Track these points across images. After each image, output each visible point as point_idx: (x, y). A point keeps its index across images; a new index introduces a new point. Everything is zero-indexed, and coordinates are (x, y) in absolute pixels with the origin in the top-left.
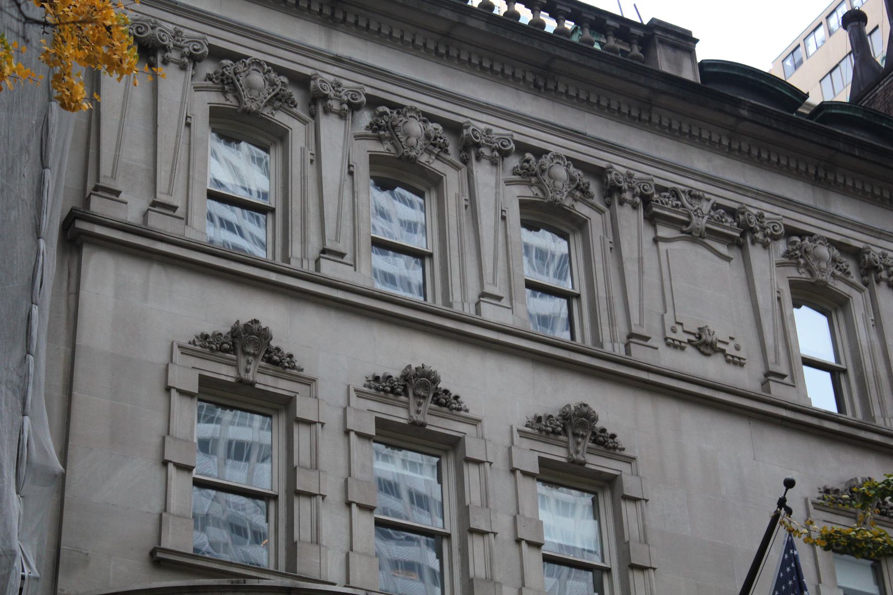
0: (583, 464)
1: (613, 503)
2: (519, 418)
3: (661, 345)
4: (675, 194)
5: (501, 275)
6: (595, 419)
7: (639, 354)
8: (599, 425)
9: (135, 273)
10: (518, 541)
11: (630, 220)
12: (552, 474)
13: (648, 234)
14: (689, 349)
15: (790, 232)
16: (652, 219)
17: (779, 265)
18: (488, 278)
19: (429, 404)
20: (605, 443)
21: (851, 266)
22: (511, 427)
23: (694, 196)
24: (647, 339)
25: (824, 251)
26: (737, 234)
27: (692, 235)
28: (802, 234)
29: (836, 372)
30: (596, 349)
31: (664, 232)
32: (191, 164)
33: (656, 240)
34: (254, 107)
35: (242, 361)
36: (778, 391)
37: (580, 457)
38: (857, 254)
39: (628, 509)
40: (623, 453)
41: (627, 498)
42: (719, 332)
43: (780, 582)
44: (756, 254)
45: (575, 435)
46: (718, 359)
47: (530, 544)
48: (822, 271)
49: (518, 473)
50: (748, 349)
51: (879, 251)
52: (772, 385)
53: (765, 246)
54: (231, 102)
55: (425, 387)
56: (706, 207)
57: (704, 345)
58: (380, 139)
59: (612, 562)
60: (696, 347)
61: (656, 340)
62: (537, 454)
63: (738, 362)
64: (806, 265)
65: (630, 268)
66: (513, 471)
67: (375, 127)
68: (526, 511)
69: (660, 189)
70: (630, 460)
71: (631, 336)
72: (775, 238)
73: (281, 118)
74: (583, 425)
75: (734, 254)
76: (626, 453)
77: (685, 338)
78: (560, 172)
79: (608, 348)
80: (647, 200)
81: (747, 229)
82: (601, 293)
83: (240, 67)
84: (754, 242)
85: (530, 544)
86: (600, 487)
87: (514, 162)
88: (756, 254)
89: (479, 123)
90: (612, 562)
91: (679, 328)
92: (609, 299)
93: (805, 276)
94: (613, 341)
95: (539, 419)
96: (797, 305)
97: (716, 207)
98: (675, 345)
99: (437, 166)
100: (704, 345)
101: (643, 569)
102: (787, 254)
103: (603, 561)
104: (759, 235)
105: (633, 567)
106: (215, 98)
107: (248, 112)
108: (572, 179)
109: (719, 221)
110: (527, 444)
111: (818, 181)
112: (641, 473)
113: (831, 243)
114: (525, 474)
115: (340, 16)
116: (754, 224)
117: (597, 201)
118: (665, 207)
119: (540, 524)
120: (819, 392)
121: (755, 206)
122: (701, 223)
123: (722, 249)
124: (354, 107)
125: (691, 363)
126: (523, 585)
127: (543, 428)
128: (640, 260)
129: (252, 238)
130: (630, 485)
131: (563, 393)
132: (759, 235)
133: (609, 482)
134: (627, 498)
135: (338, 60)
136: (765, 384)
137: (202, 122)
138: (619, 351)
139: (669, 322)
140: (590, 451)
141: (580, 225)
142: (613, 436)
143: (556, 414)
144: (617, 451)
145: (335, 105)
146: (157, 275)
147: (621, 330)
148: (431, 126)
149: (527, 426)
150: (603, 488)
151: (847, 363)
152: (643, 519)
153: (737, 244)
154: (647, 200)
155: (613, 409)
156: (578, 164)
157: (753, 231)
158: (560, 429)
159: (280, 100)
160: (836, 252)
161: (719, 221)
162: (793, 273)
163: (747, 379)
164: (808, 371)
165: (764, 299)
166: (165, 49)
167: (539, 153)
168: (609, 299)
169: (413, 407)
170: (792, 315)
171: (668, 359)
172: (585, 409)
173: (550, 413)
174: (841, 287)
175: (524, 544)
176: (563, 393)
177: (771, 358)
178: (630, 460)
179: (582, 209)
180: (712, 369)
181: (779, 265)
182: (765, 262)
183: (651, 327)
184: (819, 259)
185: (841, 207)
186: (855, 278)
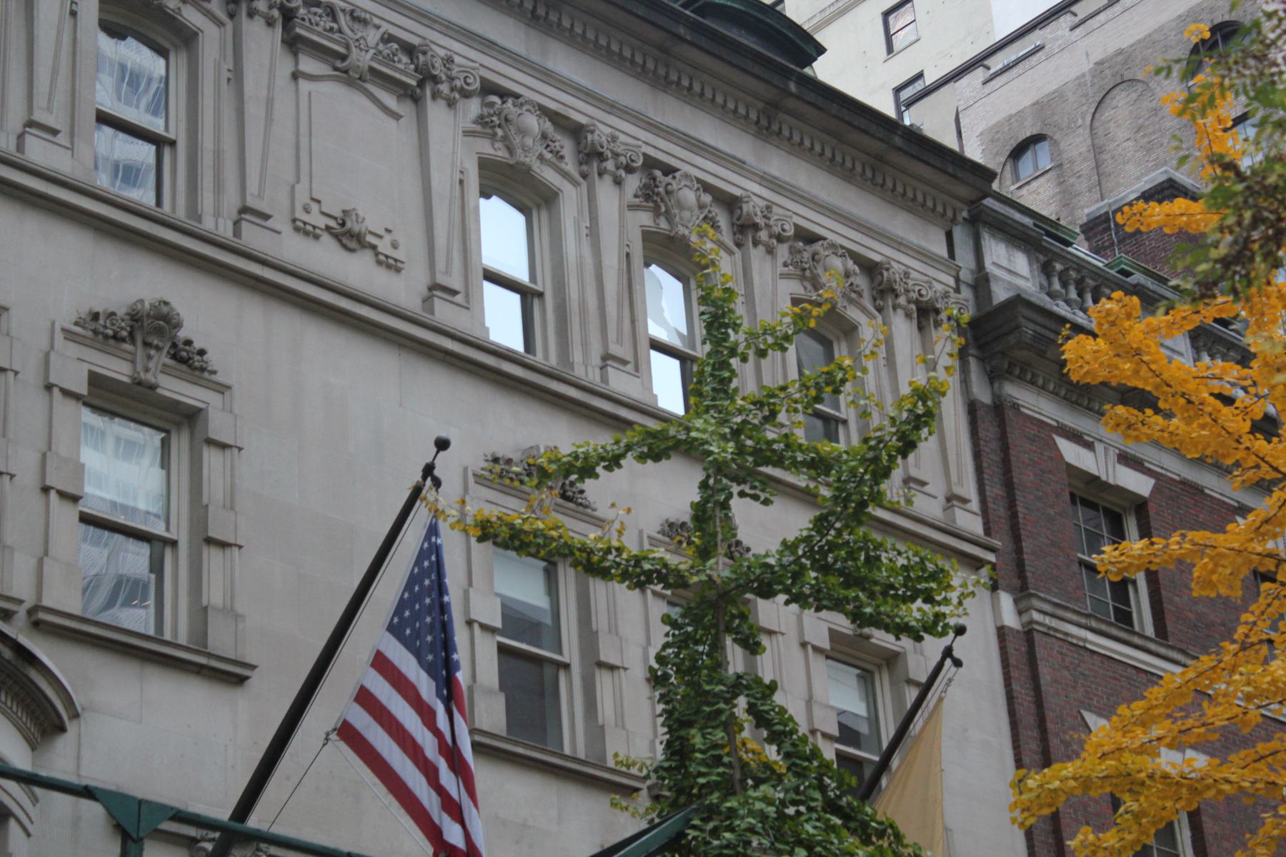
0: (153, 387)
1: (192, 448)
3: (286, 229)
5: (61, 98)
6: (178, 325)
7: (253, 237)
8: (182, 334)
10: (46, 490)
12: (105, 397)
13: (285, 66)
14: (326, 238)
15: (488, 89)
16: (293, 44)
17: (467, 133)
20: (188, 360)
21: (566, 146)
22: (53, 323)
24: (266, 217)
25: (533, 122)
27: (350, 77)
28: (504, 94)
29: (528, 295)
30: (191, 224)
31: (309, 64)
33: (296, 76)
36: (444, 313)
37: (150, 377)
38: (576, 132)
39: (212, 458)
40: (213, 377)
41: (211, 442)
42: (371, 220)
43: (413, 580)
44: (436, 112)
45: (147, 344)
46: (366, 257)
47: (62, 495)
48: (526, 150)
49: (56, 390)
50: (410, 249)
51: (608, 130)
52: (438, 304)
53: (451, 104)
56: (373, 37)
57: (348, 235)
59: (180, 532)
60: (336, 236)
61: (280, 222)
62: (86, 367)
63: (393, 266)
64: (505, 138)
65: (254, 111)
66: (49, 387)
68: (62, 446)
70: (222, 389)
71: (245, 210)
72: (466, 95)
74: (159, 332)
75: (406, 109)
76: (218, 378)
77: (322, 222)
79: (208, 224)
81: (427, 77)
82: (207, 142)
84: (435, 95)
85: (62, 495)
86: (176, 421)
88: (436, 112)
90: (180, 532)
91: (314, 207)
92: (218, 154)
93: (501, 153)
94: (217, 214)
95: (95, 316)
96: (486, 194)
97: (388, 39)
100: (348, 235)
101: (223, 545)
102: (481, 120)
103: (168, 529)
104: (444, 88)
105: (210, 541)
109: (389, 60)
110: (73, 350)
111: (534, 20)
112: (236, 411)
113: (544, 112)
114: (66, 393)
116: (439, 71)
119: (80, 468)
120: (502, 321)
121: (442, 45)
122: (361, 59)
123: (390, 100)
125: (326, 259)
126: (46, 553)
127: (101, 330)
128: (270, 102)
130: (218, 425)
131: (138, 282)
132: (444, 88)
133: (189, 417)
134: (211, 442)
136: (427, 301)
138: (225, 230)
139: (302, 197)
140: (165, 370)
141: (187, 38)
142: (202, 352)
143: (121, 312)
144: (206, 375)
147: (231, 201)
149: (76, 324)
150: (178, 425)
151: (545, 284)
152: (232, 476)
153: (412, 96)
155: (205, 312)
157: (435, 80)
158: (124, 333)
160: (548, 125)
161: (389, 60)
163: (404, 291)
164: (489, 289)
165: (441, 181)
170: (477, 209)
171: (293, 250)
172: (165, 309)
173: (111, 309)
174: (549, 176)
175: (53, 494)
176: (138, 282)
177: (440, 264)
178: (222, 389)
180: (355, 271)
181: (467, 133)
182: (448, 127)
183: (274, 201)
184: (523, 132)
185: (566, 62)
186: (570, 165)
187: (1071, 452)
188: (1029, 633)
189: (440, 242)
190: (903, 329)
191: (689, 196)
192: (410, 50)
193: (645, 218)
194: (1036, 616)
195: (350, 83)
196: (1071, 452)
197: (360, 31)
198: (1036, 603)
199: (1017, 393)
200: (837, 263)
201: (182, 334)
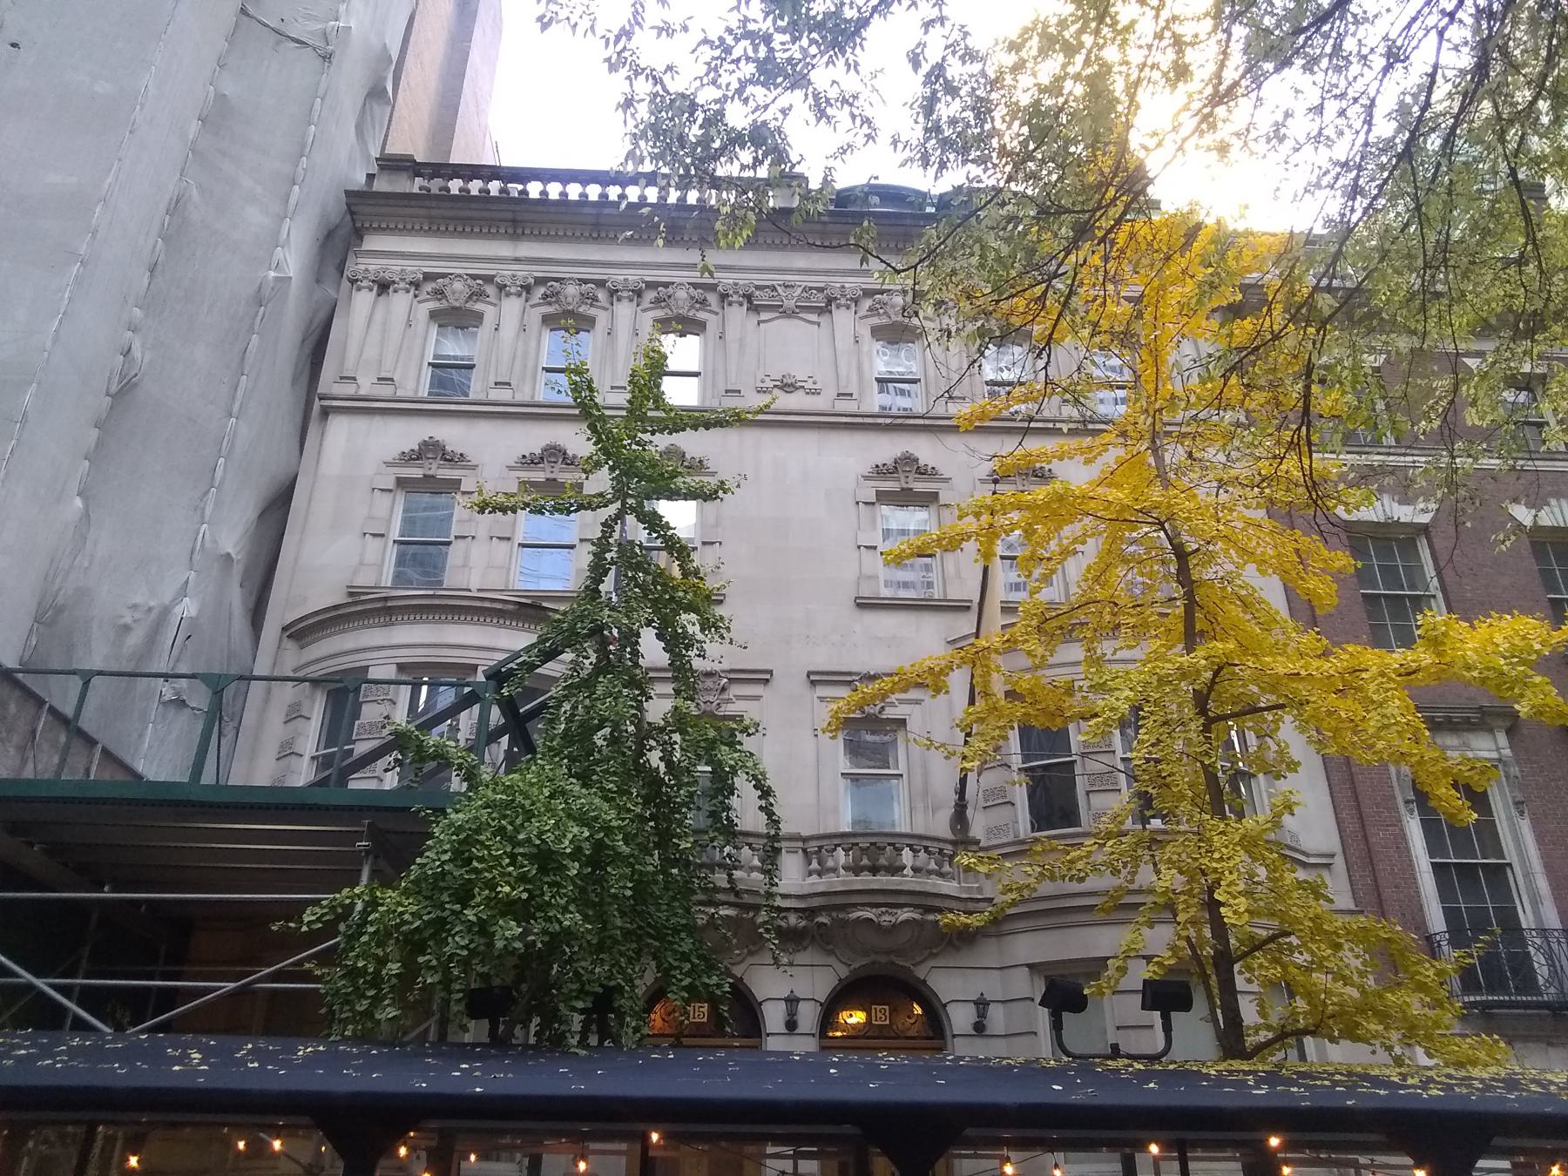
4: (774, 289)
9: (360, 424)
11: (737, 315)
16: (755, 309)
19: (559, 465)
31: (764, 316)
35: (426, 463)
54: (444, 304)
55: (554, 455)
57: (788, 387)
58: (550, 304)
60: (780, 388)
63: (816, 392)
67: (545, 296)
69: (758, 288)
73: (479, 307)
75: (824, 320)
78: (682, 294)
80: (749, 297)
83: (447, 281)
87: (650, 295)
89: (617, 276)
93: (885, 320)
99: (592, 312)
100: (788, 387)
106: (433, 305)
107: (454, 308)
115: (519, 231)
117: (715, 307)
118: (762, 298)
121: (837, 282)
123: (813, 317)
124: (527, 288)
135: (517, 260)
139: (760, 376)
145: (513, 290)
146: (378, 422)
154: (749, 297)
156: (695, 286)
159: (479, 295)
162: (876, 321)
167: (666, 285)
169: (548, 469)
179: (702, 315)
182: (843, 319)
184: (893, 307)
189: (843, 372)
192: (821, 290)
195: (789, 317)
197: (789, 291)
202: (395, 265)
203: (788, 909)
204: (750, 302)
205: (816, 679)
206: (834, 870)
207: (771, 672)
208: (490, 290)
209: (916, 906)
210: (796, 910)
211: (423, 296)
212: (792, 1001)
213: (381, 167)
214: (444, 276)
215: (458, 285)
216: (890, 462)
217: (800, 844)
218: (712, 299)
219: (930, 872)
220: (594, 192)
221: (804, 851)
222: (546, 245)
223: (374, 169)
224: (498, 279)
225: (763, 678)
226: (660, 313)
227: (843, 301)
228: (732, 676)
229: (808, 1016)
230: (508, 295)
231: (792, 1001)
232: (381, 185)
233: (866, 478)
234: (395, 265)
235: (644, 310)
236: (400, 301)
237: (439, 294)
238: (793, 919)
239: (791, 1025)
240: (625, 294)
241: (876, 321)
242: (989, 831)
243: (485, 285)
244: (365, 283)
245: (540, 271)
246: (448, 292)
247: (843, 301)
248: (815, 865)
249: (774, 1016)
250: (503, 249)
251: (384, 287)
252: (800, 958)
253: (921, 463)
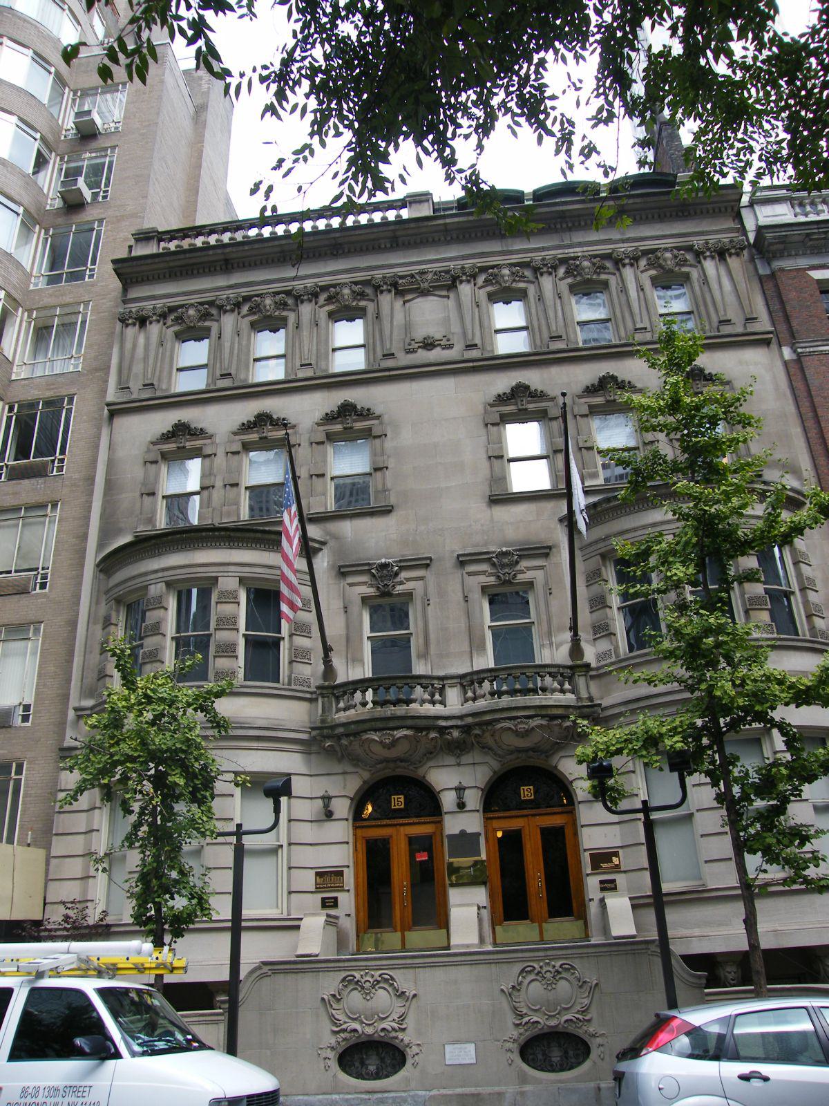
2: (318, 415)
4: (412, 276)
11: (386, 299)
14: (420, 350)
16: (400, 293)
18: (638, 319)
23: (422, 273)
26: (449, 283)
28: (493, 267)
32: (647, 305)
34: (192, 325)
46: (438, 349)
48: (505, 282)
57: (428, 344)
58: (255, 313)
63: (450, 347)
64: (497, 282)
67: (251, 309)
77: (417, 345)
78: (346, 291)
80: (395, 285)
83: (184, 310)
84: (461, 282)
98: (409, 352)
100: (428, 344)
108: (354, 292)
117: (371, 296)
123: (444, 293)
125: (423, 356)
129: (608, 336)
135: (230, 287)
137: (648, 284)
139: (408, 341)
148: (278, 298)
159: (206, 316)
161: (438, 280)
162: (489, 289)
166: (149, 317)
167: (334, 286)
168: (623, 317)
171: (404, 359)
180: (436, 355)
187: (817, 275)
188: (799, 359)
190: (710, 266)
191: (586, 263)
192: (447, 272)
193: (570, 280)
194: (799, 350)
196: (817, 275)
198: (797, 345)
199: (777, 264)
200: (668, 255)
201: (707, 372)
202: (149, 305)
203: (452, 727)
204: (396, 288)
205: (463, 561)
206: (483, 696)
207: (430, 559)
208: (214, 311)
209: (543, 717)
210: (457, 727)
211: (169, 322)
212: (460, 790)
213: (137, 240)
214: (181, 306)
215: (191, 312)
216: (508, 391)
217: (458, 680)
218: (369, 291)
219: (553, 691)
220: (294, 228)
221: (461, 684)
222: (246, 274)
223: (132, 242)
224: (218, 302)
225: (426, 563)
226: (331, 307)
227: (464, 278)
228: (402, 564)
229: (473, 799)
230: (225, 312)
231: (460, 790)
232: (140, 251)
233: (492, 405)
234: (149, 305)
235: (320, 307)
236: (154, 329)
237: (179, 320)
238: (456, 734)
239: (461, 805)
240: (305, 297)
241: (489, 289)
242: (600, 657)
243: (212, 309)
244: (130, 321)
245: (245, 291)
246: (185, 317)
247: (464, 278)
248: (470, 694)
249: (448, 800)
250: (221, 281)
251: (143, 321)
252: (466, 759)
253: (533, 388)
